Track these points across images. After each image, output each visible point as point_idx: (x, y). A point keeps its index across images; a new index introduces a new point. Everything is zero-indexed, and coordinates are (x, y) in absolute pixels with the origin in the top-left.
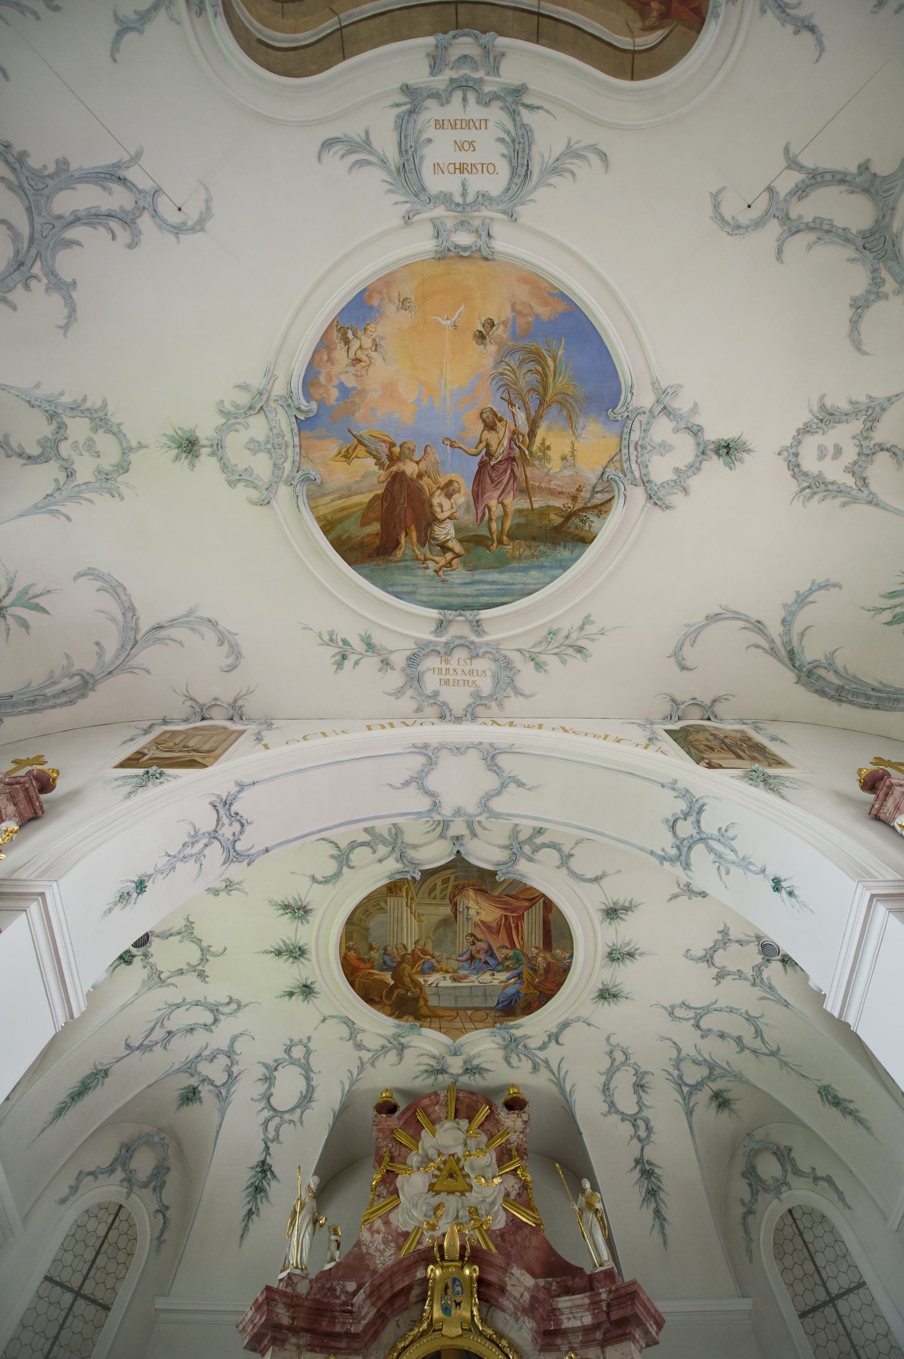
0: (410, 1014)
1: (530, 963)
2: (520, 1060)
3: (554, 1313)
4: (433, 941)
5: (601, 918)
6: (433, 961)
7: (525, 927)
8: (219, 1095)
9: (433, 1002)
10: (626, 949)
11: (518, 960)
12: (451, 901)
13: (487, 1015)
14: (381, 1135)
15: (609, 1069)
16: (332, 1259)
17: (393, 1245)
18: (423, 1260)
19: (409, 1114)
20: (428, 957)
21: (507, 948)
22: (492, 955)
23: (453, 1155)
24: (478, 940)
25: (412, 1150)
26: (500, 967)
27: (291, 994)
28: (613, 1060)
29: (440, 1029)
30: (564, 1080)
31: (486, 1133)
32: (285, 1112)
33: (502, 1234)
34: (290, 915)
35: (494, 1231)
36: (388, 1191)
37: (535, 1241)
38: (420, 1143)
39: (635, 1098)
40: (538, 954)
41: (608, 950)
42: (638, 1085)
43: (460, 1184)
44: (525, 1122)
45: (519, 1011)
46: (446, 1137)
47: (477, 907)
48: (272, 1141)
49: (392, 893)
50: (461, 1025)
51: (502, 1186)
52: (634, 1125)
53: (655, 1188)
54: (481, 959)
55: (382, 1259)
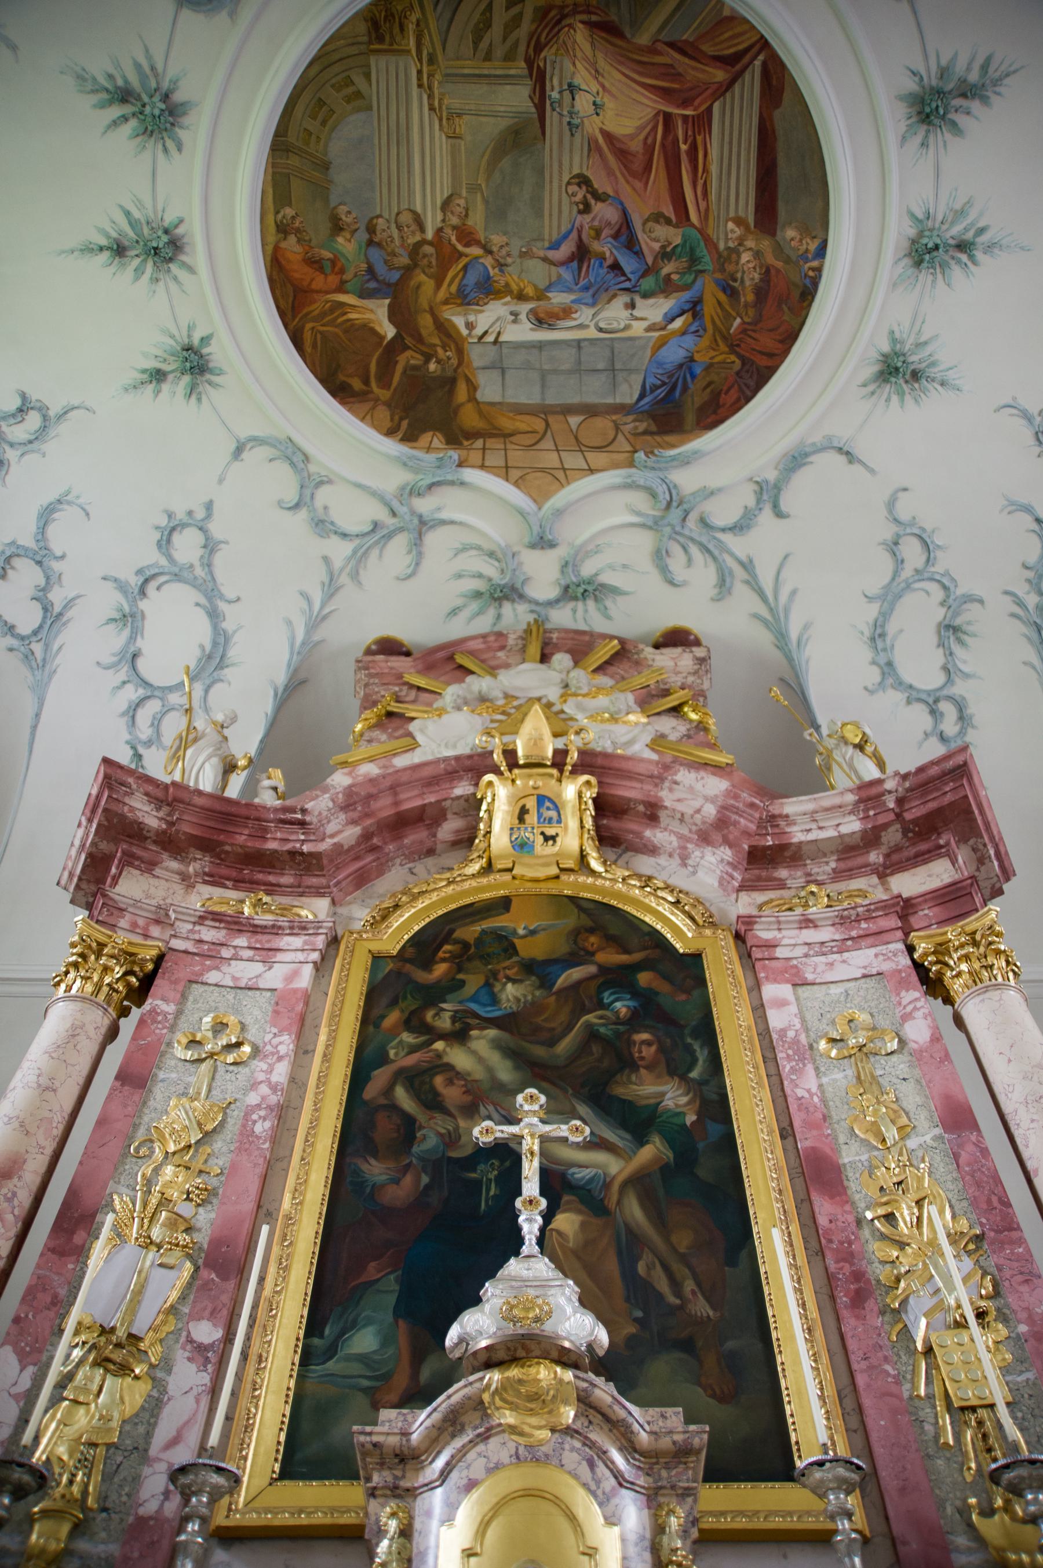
0: (435, 428)
1: (722, 270)
2: (690, 561)
4: (486, 202)
5: (903, 129)
6: (488, 261)
7: (714, 153)
8: (28, 657)
9: (489, 391)
10: (956, 230)
11: (694, 260)
12: (530, 63)
13: (617, 429)
15: (887, 587)
20: (475, 251)
21: (668, 222)
22: (631, 244)
23: (539, 699)
24: (599, 197)
26: (648, 283)
27: (158, 376)
28: (899, 563)
29: (505, 472)
30: (787, 611)
34: (133, 123)
39: (938, 657)
40: (741, 241)
41: (912, 232)
42: (948, 627)
45: (690, 418)
47: (594, 87)
48: (149, 744)
49: (380, 39)
50: (551, 459)
52: (933, 712)
54: (602, 258)
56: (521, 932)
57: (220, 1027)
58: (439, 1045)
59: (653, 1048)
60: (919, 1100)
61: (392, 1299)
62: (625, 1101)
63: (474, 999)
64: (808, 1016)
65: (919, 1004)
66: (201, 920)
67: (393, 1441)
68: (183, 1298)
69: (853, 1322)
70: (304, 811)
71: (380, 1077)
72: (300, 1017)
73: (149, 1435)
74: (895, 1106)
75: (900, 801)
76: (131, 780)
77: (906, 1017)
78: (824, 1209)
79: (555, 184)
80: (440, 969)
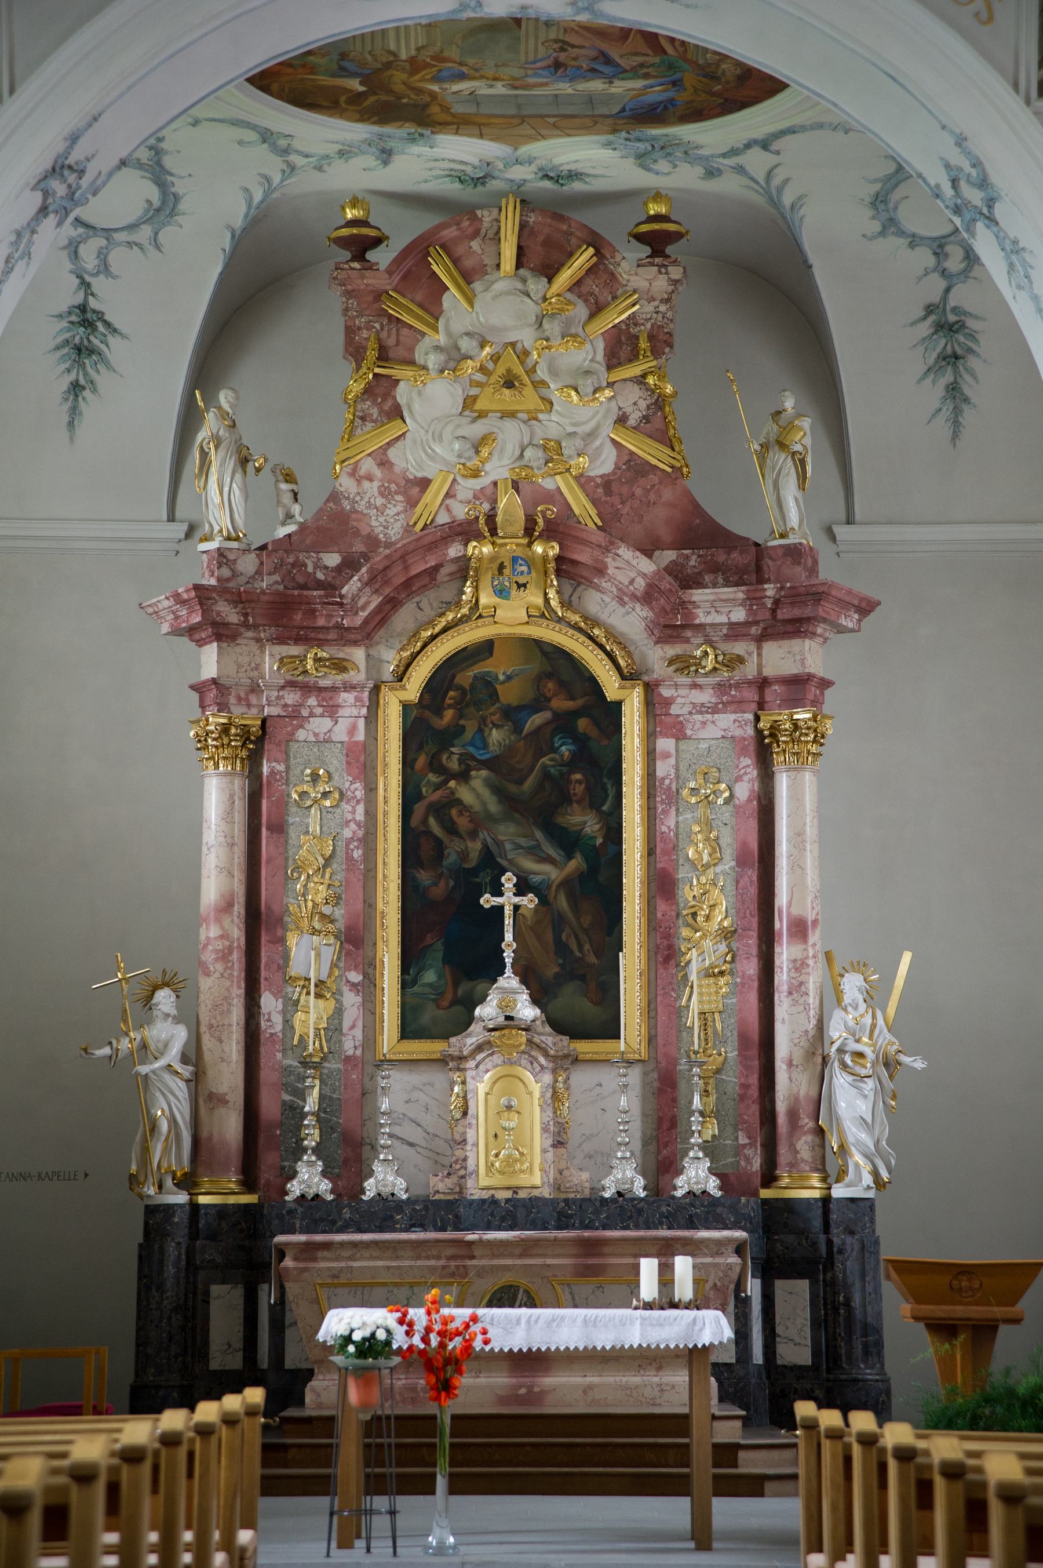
3: (685, 607)
14: (353, 303)
16: (289, 517)
18: (459, 534)
19: (409, 263)
23: (513, 345)
25: (423, 334)
30: (780, 190)
31: (586, 301)
32: (116, 230)
33: (607, 483)
35: (591, 479)
36: (381, 411)
37: (668, 494)
43: (530, 399)
44: (675, 282)
46: (497, 308)
51: (613, 404)
52: (935, 254)
53: (959, 351)
56: (501, 678)
57: (315, 778)
58: (452, 784)
59: (583, 786)
60: (729, 840)
61: (440, 955)
62: (562, 827)
63: (472, 743)
64: (681, 767)
65: (749, 770)
66: (283, 688)
67: (457, 1053)
68: (339, 959)
69: (662, 971)
70: (341, 597)
71: (419, 809)
72: (363, 761)
73: (340, 1024)
74: (714, 844)
75: (777, 602)
77: (739, 779)
78: (662, 907)
79: (532, 41)
80: (449, 714)
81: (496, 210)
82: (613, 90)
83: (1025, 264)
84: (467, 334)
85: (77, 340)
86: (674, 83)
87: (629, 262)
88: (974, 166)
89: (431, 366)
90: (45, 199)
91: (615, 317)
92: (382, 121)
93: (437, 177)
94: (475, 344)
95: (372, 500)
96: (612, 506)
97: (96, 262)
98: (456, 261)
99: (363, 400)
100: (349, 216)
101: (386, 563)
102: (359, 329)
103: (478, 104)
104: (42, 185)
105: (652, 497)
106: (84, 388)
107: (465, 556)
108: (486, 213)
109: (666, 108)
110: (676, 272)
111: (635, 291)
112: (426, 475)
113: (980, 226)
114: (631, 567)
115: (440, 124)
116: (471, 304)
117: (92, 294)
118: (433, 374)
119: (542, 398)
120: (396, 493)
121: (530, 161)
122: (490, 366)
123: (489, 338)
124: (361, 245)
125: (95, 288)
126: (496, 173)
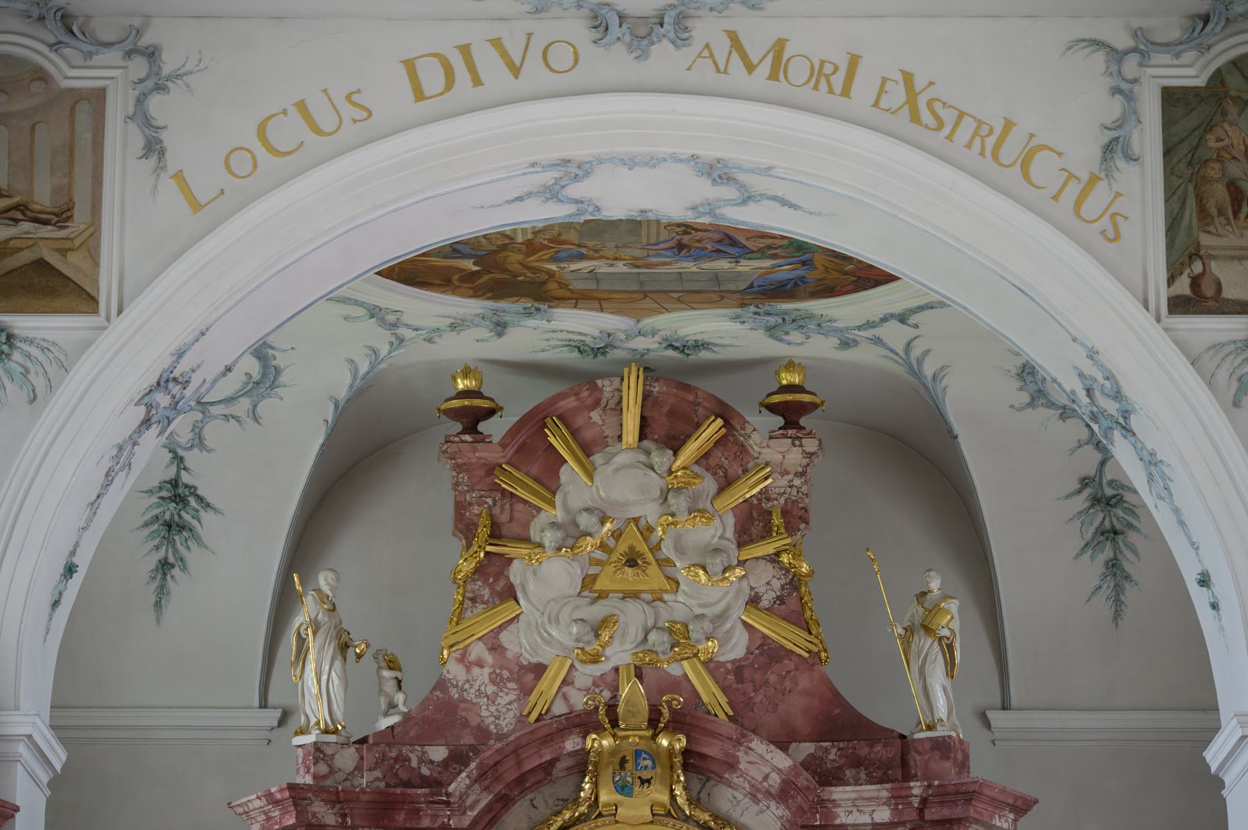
3: (823, 804)
16: (392, 706)
17: (512, 685)
18: (578, 726)
23: (636, 520)
25: (539, 510)
30: (920, 361)
31: (714, 474)
32: (213, 403)
33: (738, 669)
35: (722, 664)
36: (493, 592)
37: (805, 681)
38: (558, 499)
43: (654, 578)
44: (811, 455)
46: (620, 482)
51: (745, 584)
53: (1118, 526)
55: (492, 709)
70: (448, 795)
75: (924, 801)
76: (310, 795)
81: (618, 380)
82: (740, 269)
83: (1164, 476)
84: (587, 510)
85: (167, 516)
86: (804, 263)
87: (760, 426)
88: (1107, 378)
89: (547, 544)
90: (148, 412)
91: (746, 490)
92: (496, 297)
93: (555, 347)
94: (594, 520)
95: (482, 688)
96: (744, 694)
97: (191, 436)
98: (574, 433)
99: (474, 580)
100: (461, 386)
101: (497, 758)
102: (470, 504)
103: (598, 281)
104: (146, 400)
105: (788, 684)
106: (173, 566)
107: (583, 749)
108: (606, 382)
109: (796, 285)
110: (810, 445)
111: (767, 464)
112: (541, 660)
113: (1117, 434)
114: (766, 762)
115: (559, 299)
116: (591, 478)
117: (185, 469)
118: (550, 553)
119: (668, 578)
120: (509, 680)
121: (654, 333)
122: (611, 543)
123: (609, 514)
124: (472, 417)
125: (188, 463)
126: (618, 344)
